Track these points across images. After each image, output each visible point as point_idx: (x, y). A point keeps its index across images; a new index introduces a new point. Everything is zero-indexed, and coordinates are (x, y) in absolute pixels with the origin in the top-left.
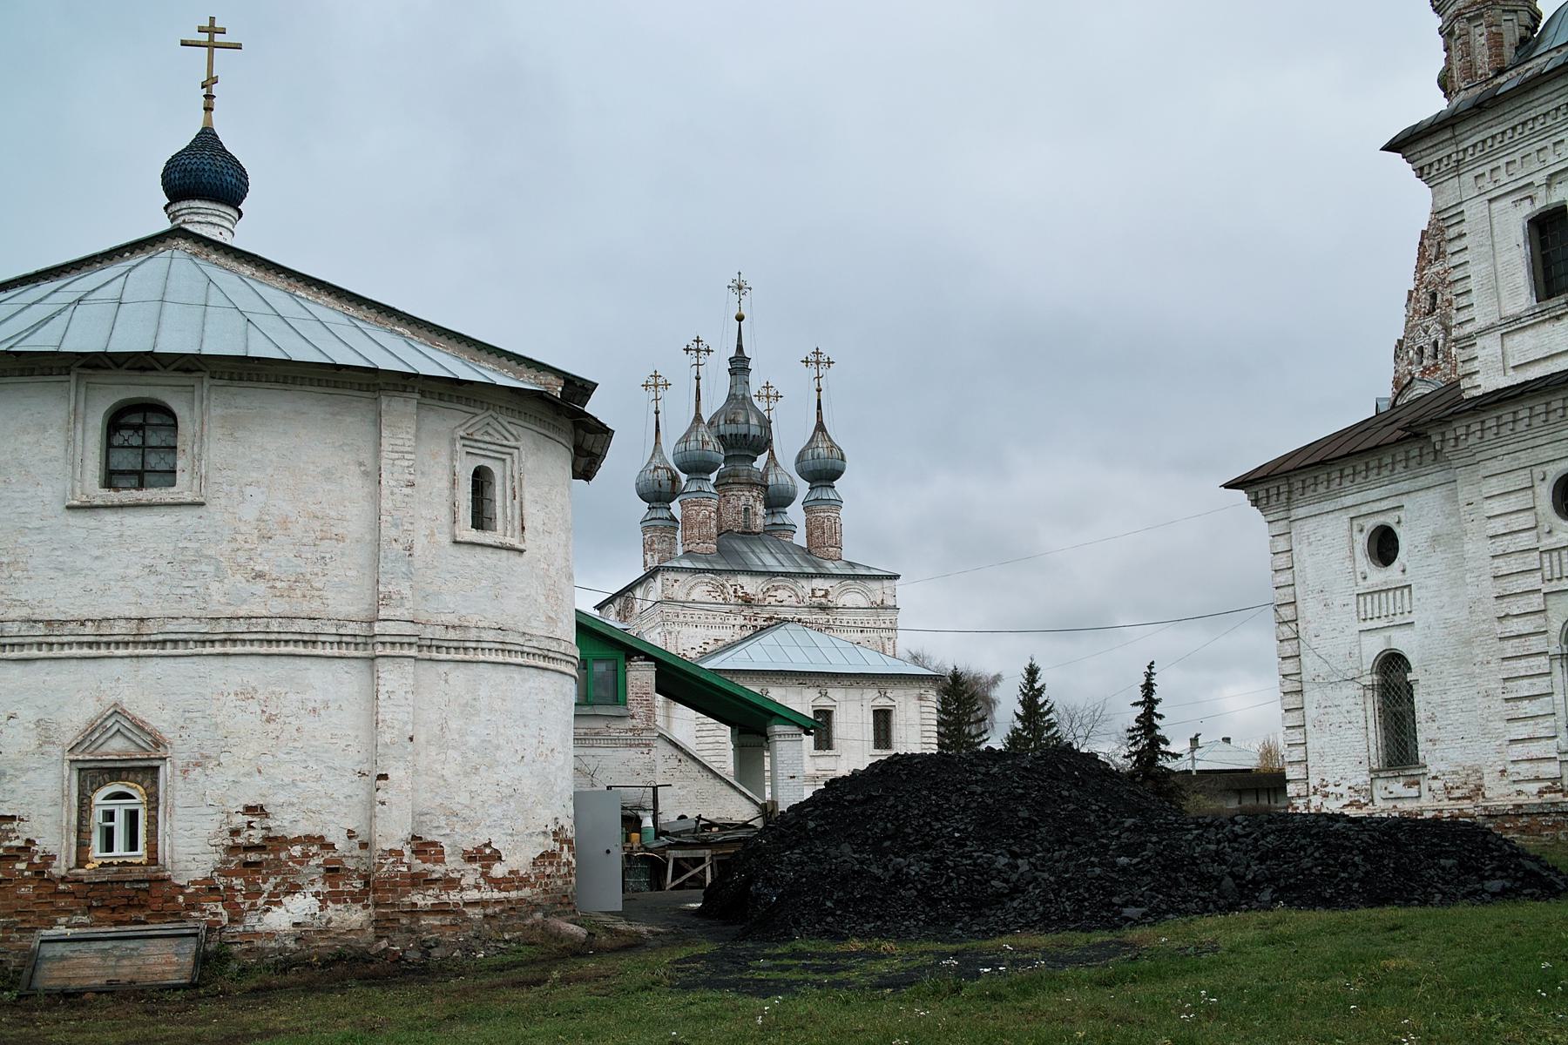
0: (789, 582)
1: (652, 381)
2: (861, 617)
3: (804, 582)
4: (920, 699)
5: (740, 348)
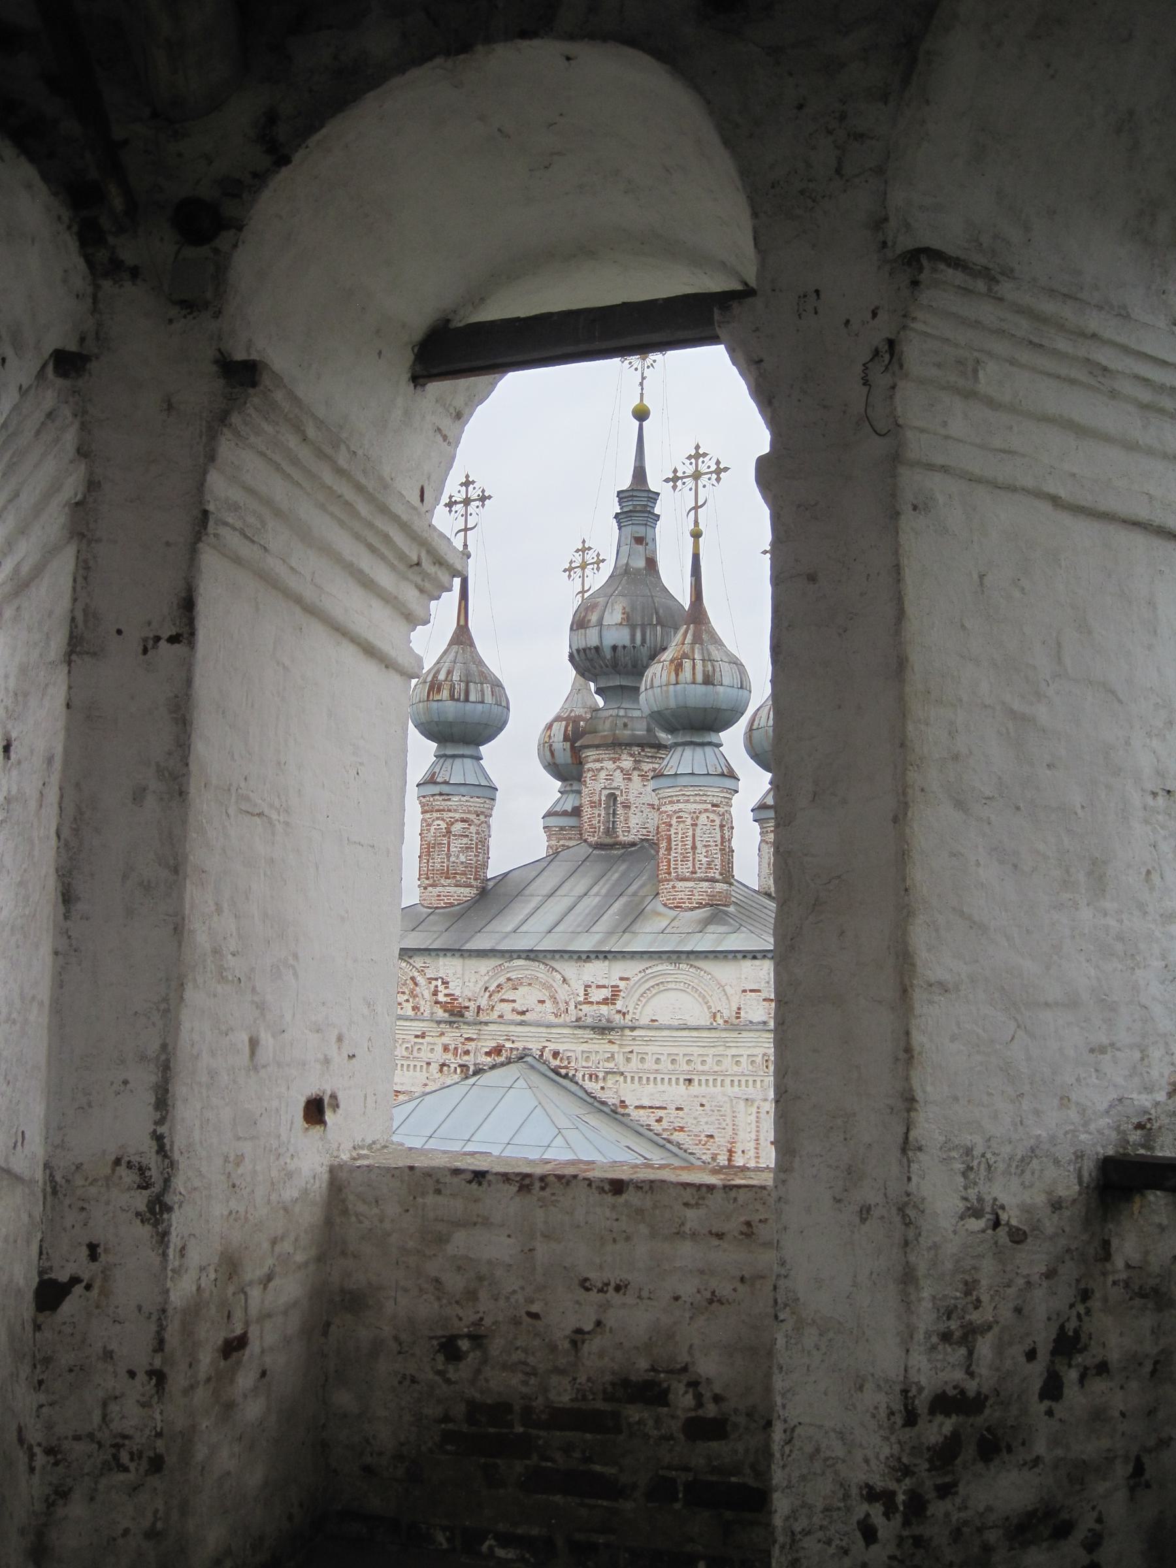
0: (538, 970)
1: (578, 559)
3: (569, 969)
5: (640, 474)
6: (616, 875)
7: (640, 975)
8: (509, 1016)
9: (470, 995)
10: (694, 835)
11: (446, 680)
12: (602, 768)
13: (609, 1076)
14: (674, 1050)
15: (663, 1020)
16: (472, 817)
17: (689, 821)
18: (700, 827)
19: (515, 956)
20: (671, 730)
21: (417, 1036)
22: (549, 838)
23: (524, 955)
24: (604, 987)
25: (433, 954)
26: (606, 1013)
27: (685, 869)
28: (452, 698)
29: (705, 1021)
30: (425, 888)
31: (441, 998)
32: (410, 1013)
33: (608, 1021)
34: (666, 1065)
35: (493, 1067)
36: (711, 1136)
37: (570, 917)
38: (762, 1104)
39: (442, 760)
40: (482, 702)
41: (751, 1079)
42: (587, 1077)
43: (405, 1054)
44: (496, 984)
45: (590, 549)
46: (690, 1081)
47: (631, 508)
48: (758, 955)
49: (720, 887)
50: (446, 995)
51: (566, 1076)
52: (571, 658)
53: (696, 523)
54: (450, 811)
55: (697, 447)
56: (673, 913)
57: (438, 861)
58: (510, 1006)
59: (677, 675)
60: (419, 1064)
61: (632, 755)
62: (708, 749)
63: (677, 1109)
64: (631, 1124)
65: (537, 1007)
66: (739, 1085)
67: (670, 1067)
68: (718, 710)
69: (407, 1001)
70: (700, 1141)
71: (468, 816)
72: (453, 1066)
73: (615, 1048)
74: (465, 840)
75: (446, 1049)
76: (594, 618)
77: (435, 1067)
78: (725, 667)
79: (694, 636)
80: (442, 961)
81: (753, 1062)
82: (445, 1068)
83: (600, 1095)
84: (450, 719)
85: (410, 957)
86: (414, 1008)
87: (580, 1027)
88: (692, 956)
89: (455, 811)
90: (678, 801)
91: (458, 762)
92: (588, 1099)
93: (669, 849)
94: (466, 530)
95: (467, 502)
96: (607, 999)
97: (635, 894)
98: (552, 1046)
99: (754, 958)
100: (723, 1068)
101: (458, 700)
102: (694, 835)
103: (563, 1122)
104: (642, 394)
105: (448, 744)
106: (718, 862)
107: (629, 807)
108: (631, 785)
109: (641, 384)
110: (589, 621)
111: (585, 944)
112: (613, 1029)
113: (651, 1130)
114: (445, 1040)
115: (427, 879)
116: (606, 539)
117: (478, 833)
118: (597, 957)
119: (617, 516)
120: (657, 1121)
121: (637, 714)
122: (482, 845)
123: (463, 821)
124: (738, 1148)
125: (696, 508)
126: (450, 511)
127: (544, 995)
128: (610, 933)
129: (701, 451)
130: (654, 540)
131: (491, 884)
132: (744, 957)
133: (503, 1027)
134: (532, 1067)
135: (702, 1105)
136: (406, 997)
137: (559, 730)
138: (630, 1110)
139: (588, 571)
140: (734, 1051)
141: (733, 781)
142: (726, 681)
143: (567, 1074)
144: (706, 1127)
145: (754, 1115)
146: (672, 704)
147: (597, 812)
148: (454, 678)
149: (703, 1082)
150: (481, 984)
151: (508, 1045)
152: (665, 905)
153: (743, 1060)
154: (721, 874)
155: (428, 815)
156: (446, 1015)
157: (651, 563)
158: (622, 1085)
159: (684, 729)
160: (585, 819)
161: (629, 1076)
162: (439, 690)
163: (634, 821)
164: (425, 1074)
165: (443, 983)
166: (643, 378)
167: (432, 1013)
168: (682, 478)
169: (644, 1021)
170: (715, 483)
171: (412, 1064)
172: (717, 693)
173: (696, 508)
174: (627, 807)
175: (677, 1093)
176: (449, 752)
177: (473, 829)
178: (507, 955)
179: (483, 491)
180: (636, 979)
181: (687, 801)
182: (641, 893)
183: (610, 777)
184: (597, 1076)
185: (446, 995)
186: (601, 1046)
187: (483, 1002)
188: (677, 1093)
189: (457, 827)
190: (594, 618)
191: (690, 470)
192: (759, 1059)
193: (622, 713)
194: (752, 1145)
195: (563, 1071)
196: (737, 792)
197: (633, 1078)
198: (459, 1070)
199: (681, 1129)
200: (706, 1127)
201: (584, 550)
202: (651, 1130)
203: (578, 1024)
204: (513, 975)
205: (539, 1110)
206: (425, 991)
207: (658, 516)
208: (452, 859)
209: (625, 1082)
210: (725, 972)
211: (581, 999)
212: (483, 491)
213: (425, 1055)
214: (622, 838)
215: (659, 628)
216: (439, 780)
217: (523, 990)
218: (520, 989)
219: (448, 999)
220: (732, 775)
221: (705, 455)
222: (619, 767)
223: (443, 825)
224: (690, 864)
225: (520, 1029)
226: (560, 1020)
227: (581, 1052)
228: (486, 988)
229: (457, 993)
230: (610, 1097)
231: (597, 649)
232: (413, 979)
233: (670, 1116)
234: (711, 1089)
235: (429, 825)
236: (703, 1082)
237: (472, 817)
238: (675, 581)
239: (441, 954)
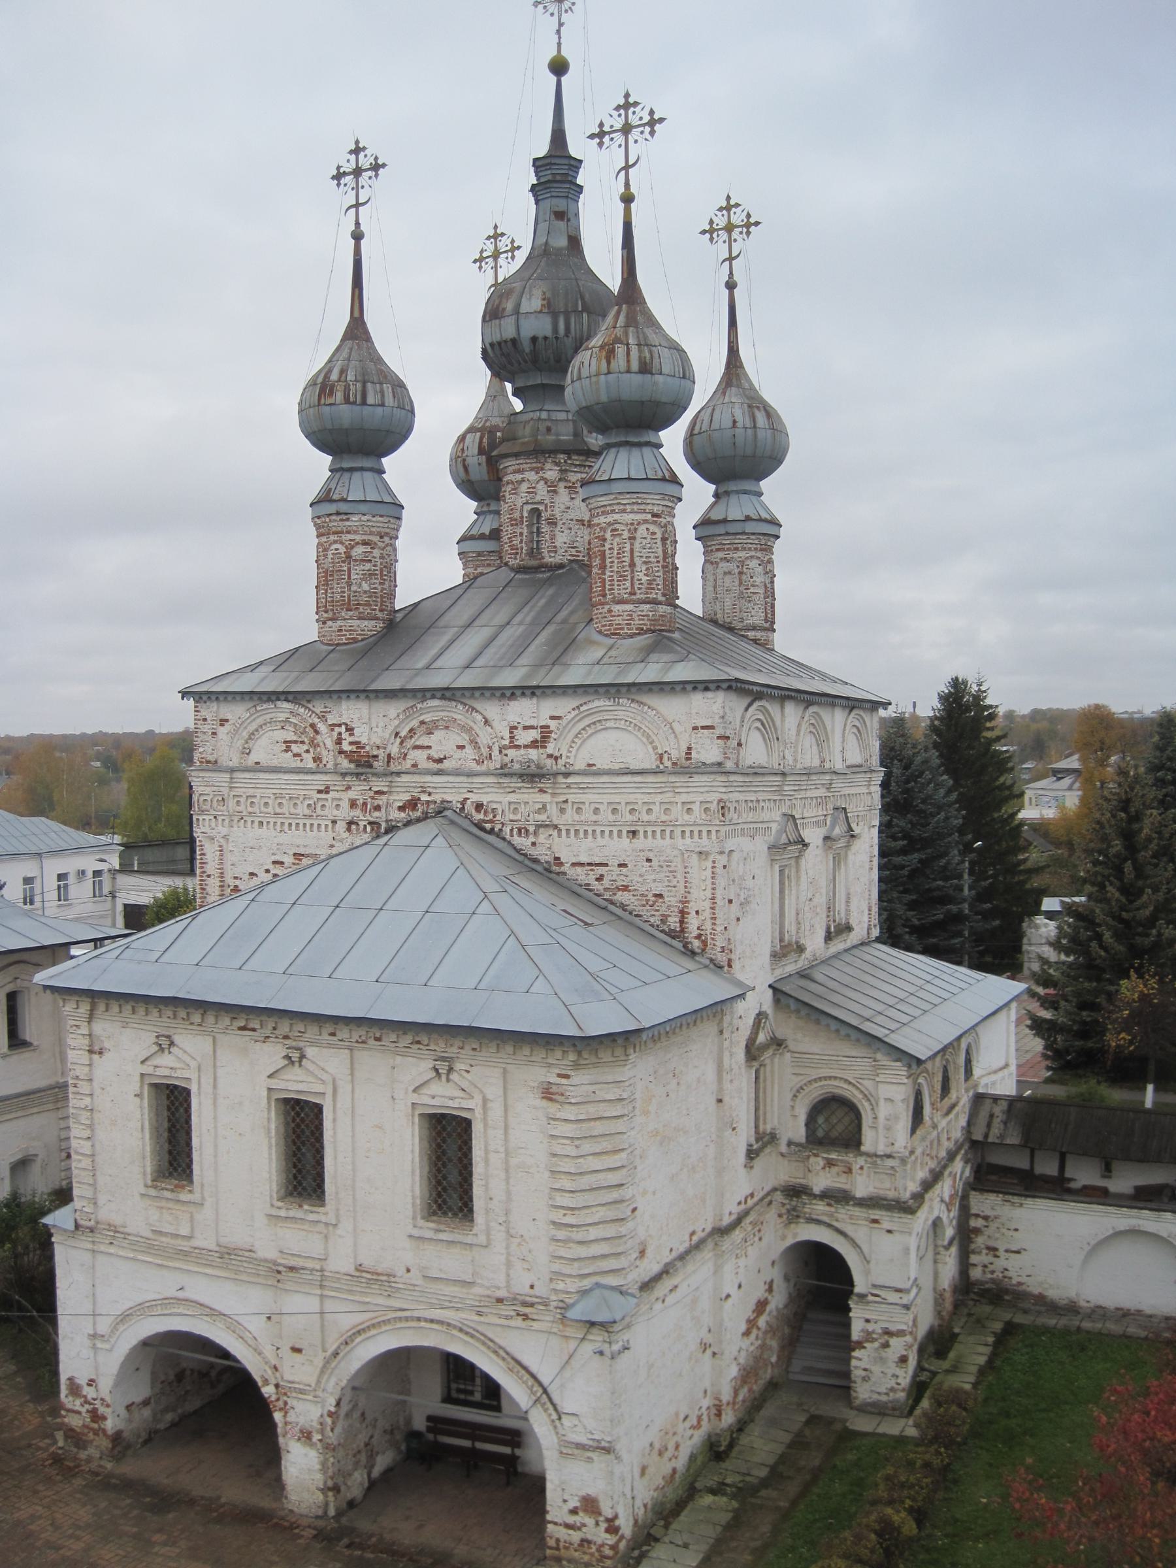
0: (457, 712)
2: (630, 793)
3: (492, 709)
4: (548, 1094)
5: (558, 137)
6: (543, 601)
7: (574, 713)
8: (424, 764)
9: (378, 742)
10: (632, 550)
11: (339, 380)
12: (523, 480)
13: (541, 830)
14: (616, 798)
15: (602, 763)
16: (375, 539)
17: (626, 534)
18: (638, 540)
19: (428, 695)
20: (603, 429)
21: (320, 792)
22: (465, 567)
23: (439, 694)
24: (532, 727)
25: (335, 696)
26: (535, 758)
27: (622, 590)
28: (347, 400)
29: (650, 763)
30: (324, 623)
31: (346, 747)
32: (311, 765)
33: (538, 766)
34: (606, 815)
35: (408, 823)
36: (660, 896)
37: (491, 651)
38: (718, 857)
39: (338, 475)
40: (383, 405)
41: (704, 829)
42: (515, 831)
43: (307, 812)
44: (407, 729)
45: (503, 234)
46: (634, 833)
47: (550, 177)
48: (711, 686)
49: (664, 609)
50: (351, 743)
51: (491, 832)
52: (485, 356)
53: (627, 185)
54: (348, 532)
55: (627, 96)
56: (610, 641)
57: (337, 590)
58: (426, 752)
59: (609, 363)
60: (323, 823)
61: (557, 464)
62: (647, 451)
63: (620, 865)
64: (567, 884)
65: (457, 752)
66: (692, 836)
67: (611, 817)
68: (657, 404)
69: (307, 751)
70: (647, 901)
71: (371, 538)
72: (362, 824)
73: (546, 798)
74: (368, 566)
75: (353, 804)
76: (509, 306)
77: (341, 826)
78: (665, 353)
79: (627, 317)
80: (344, 705)
81: (706, 810)
82: (353, 827)
83: (534, 852)
84: (346, 426)
85: (309, 701)
86: (315, 760)
87: (505, 775)
88: (633, 690)
89: (355, 532)
90: (613, 511)
91: (357, 475)
92: (521, 858)
93: (603, 567)
94: (357, 205)
95: (357, 172)
96: (536, 741)
97: (564, 621)
98: (474, 798)
99: (707, 689)
100: (672, 817)
101: (354, 403)
102: (632, 550)
103: (490, 885)
104: (559, 44)
105: (345, 456)
106: (660, 581)
107: (555, 524)
108: (557, 499)
109: (558, 32)
110: (504, 309)
111: (509, 678)
112: (543, 776)
113: (591, 890)
114: (352, 794)
115: (326, 612)
116: (520, 219)
117: (382, 557)
118: (523, 694)
119: (533, 189)
120: (597, 880)
121: (562, 416)
122: (386, 572)
123: (365, 543)
124: (692, 908)
125: (627, 168)
126: (339, 185)
127: (463, 739)
128: (536, 666)
129: (631, 100)
130: (577, 215)
131: (399, 616)
132: (695, 688)
133: (416, 778)
134: (452, 822)
135: (649, 860)
136: (305, 747)
137: (473, 441)
138: (566, 868)
139: (502, 260)
140: (684, 798)
141: (676, 487)
142: (665, 370)
143: (493, 829)
144: (653, 885)
145: (709, 871)
146: (604, 398)
147: (518, 531)
148: (349, 378)
149: (650, 834)
150: (391, 728)
151: (424, 798)
152: (600, 632)
153: (696, 807)
154: (664, 595)
155: (324, 539)
156: (352, 766)
157: (575, 242)
158: (557, 839)
159: (618, 427)
160: (505, 539)
161: (563, 828)
162: (331, 393)
163: (561, 539)
164: (330, 834)
165: (347, 730)
166: (561, 25)
167: (336, 765)
168: (609, 133)
169: (580, 765)
170: (649, 137)
171: (316, 823)
172: (655, 383)
173: (627, 168)
174: (553, 523)
175: (620, 848)
176: (346, 465)
177: (376, 553)
178: (419, 695)
179: (376, 159)
180: (570, 717)
181: (624, 511)
182: (571, 620)
183: (532, 491)
184: (527, 831)
185: (351, 743)
186: (530, 798)
187: (394, 749)
188: (620, 848)
189: (359, 551)
190: (509, 306)
191: (619, 123)
192: (714, 806)
193: (544, 415)
194: (708, 904)
195: (488, 826)
196: (680, 500)
197: (568, 831)
198: (369, 828)
199: (625, 888)
200: (653, 885)
201: (496, 236)
202: (591, 890)
203: (504, 772)
204: (427, 718)
205: (461, 871)
206: (327, 739)
207: (581, 187)
208: (354, 588)
209: (560, 836)
210: (673, 708)
211: (507, 742)
212: (376, 159)
213: (331, 812)
214: (548, 560)
215: (585, 315)
216: (334, 497)
217: (439, 735)
218: (436, 733)
219: (354, 748)
220: (674, 480)
221: (636, 104)
222: (542, 478)
223: (342, 549)
224: (628, 584)
225: (436, 779)
226: (483, 768)
227: (509, 803)
228: (397, 734)
229: (364, 740)
230: (542, 853)
231: (514, 341)
232: (313, 726)
233: (613, 874)
234: (659, 841)
235: (325, 550)
236: (650, 834)
237: (375, 539)
238: (605, 265)
239: (344, 696)
